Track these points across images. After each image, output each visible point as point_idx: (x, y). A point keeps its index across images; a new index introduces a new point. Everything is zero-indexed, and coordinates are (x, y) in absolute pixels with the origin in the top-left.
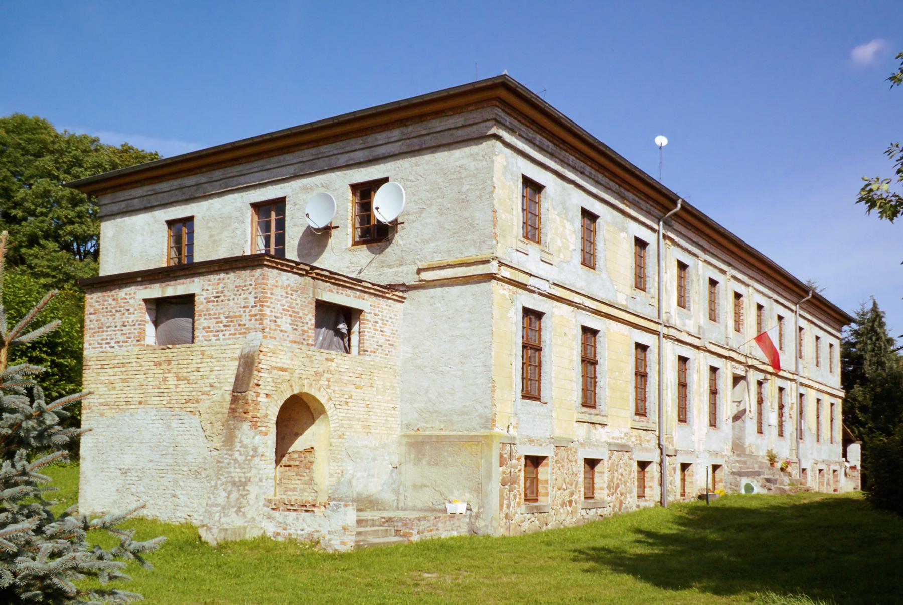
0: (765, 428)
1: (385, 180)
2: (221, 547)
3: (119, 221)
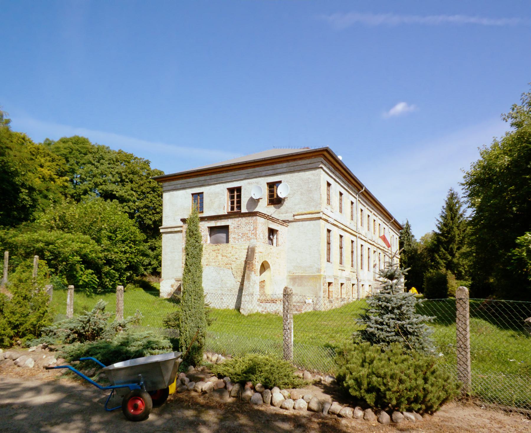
2: (250, 316)
3: (171, 193)
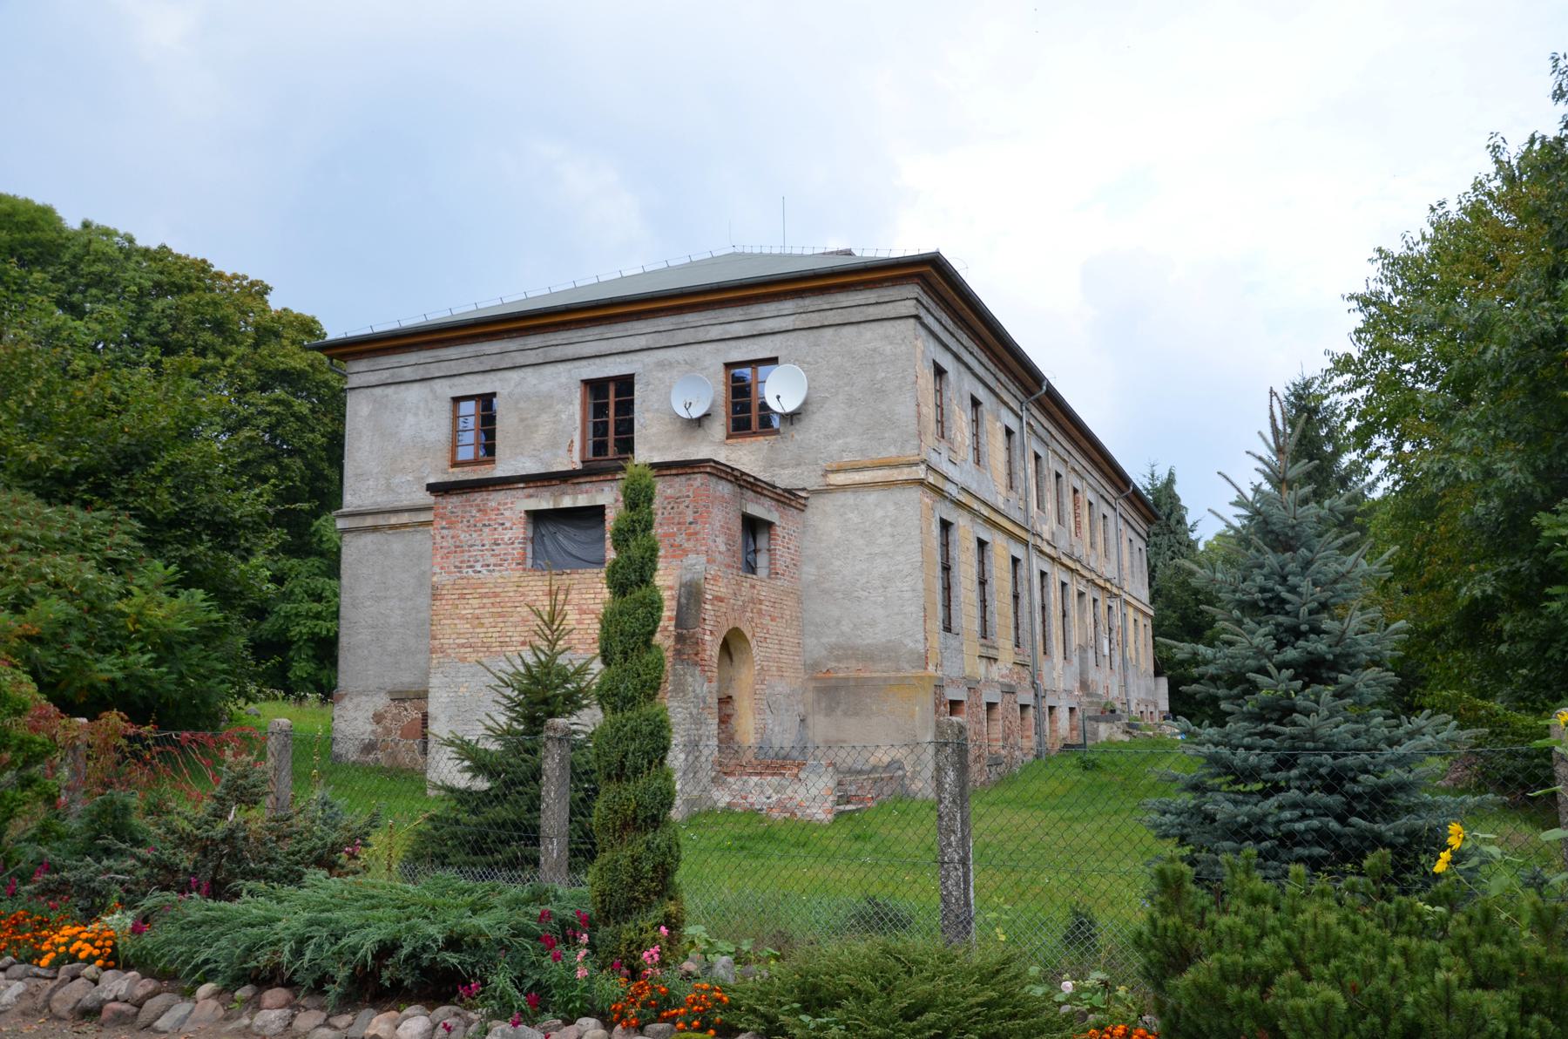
0: (1100, 658)
1: (773, 361)
